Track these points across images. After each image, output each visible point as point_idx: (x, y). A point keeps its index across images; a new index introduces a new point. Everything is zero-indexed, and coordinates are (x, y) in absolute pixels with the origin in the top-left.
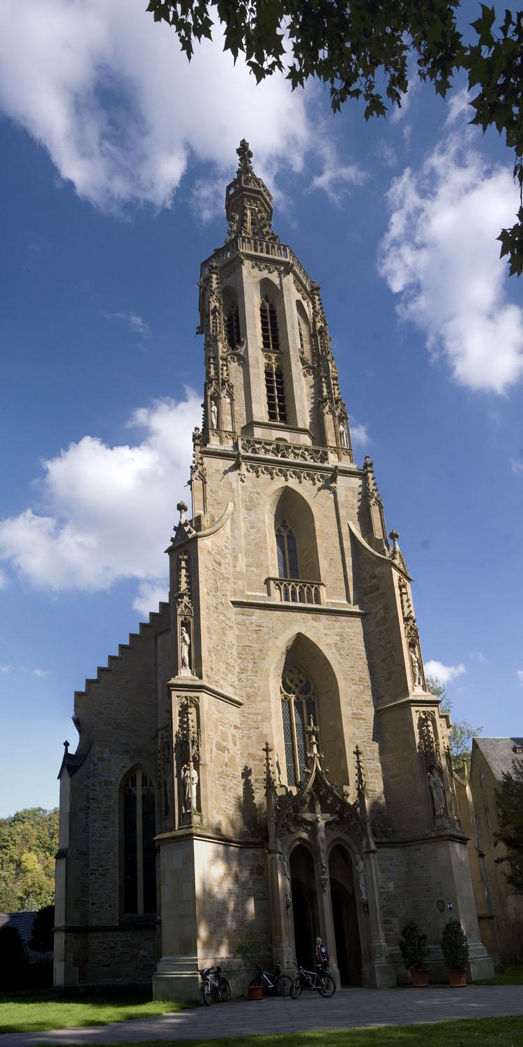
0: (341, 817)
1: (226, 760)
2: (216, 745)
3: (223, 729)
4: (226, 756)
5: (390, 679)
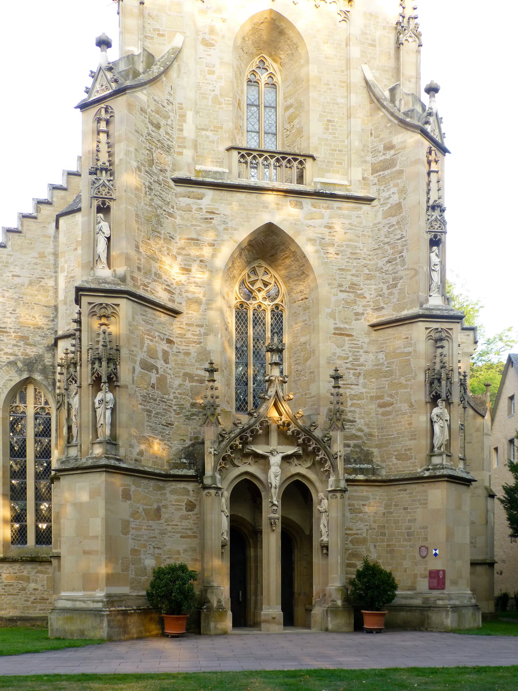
0: (304, 450)
1: (154, 381)
2: (140, 364)
3: (151, 343)
4: (154, 377)
5: (395, 286)
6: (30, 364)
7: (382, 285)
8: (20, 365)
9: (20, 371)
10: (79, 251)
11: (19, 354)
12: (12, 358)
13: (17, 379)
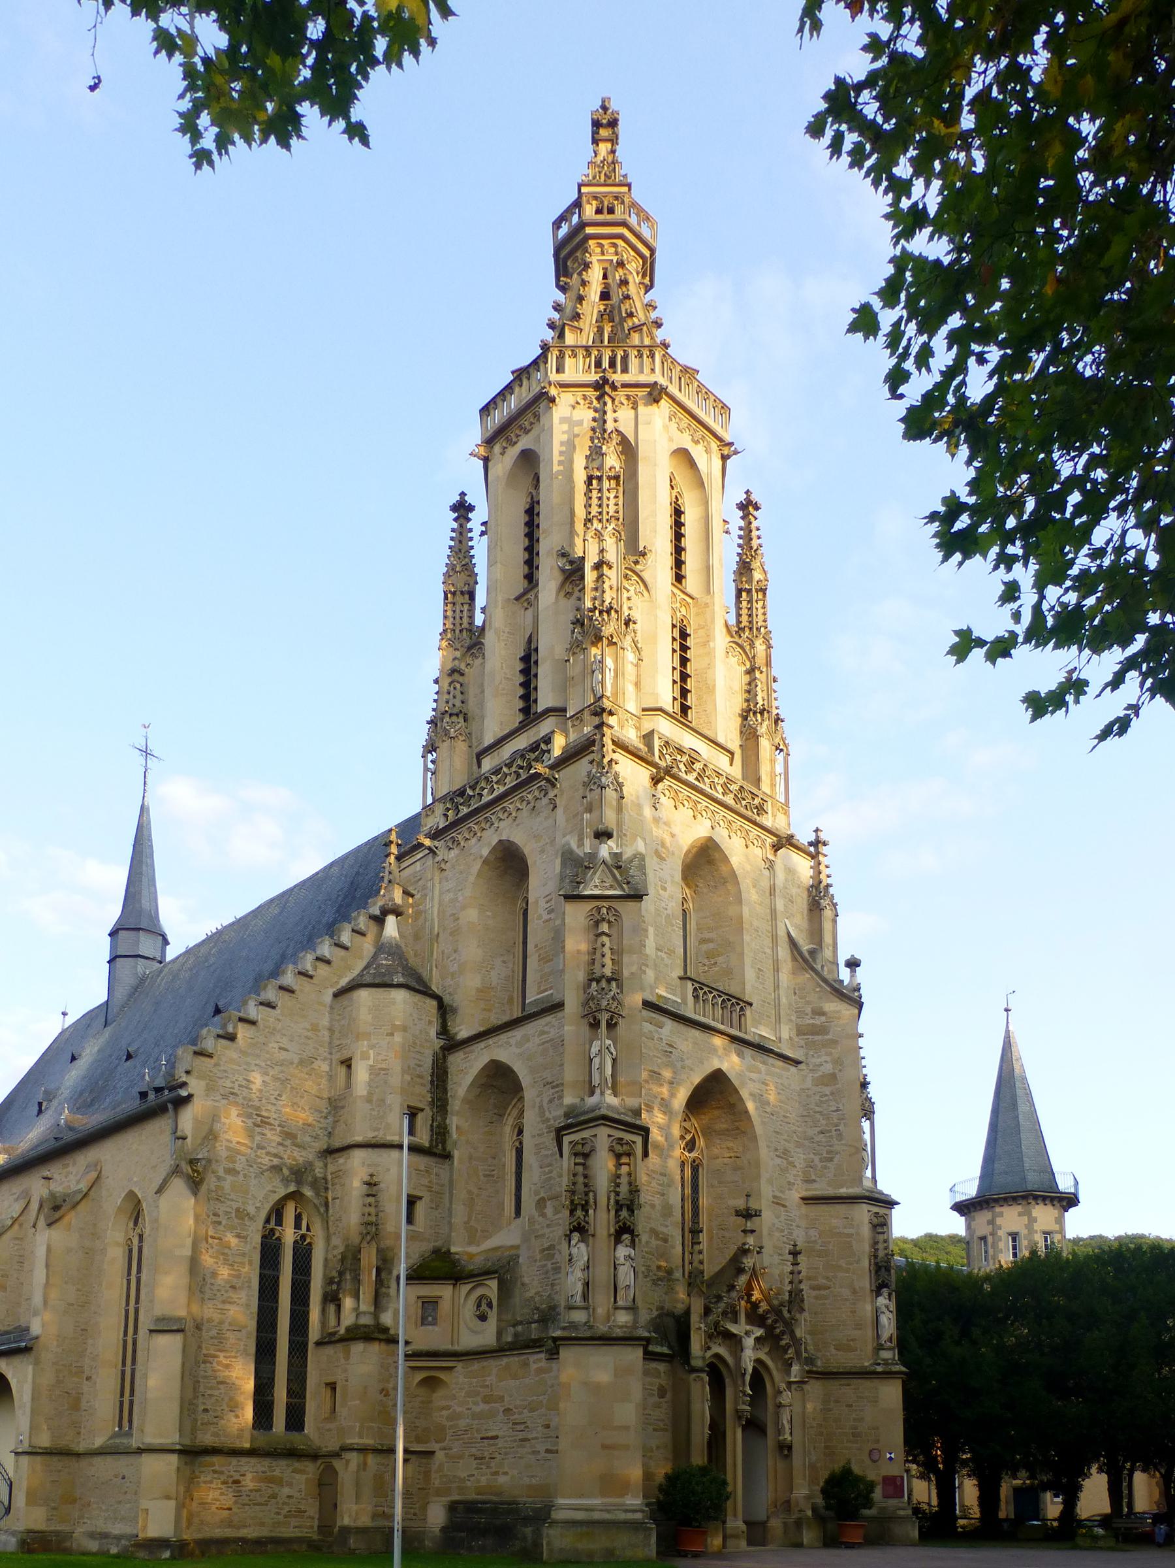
6: (299, 1174)
7: (812, 1156)
8: (286, 1172)
9: (286, 1181)
10: (398, 1038)
11: (286, 1157)
12: (276, 1161)
13: (282, 1192)
